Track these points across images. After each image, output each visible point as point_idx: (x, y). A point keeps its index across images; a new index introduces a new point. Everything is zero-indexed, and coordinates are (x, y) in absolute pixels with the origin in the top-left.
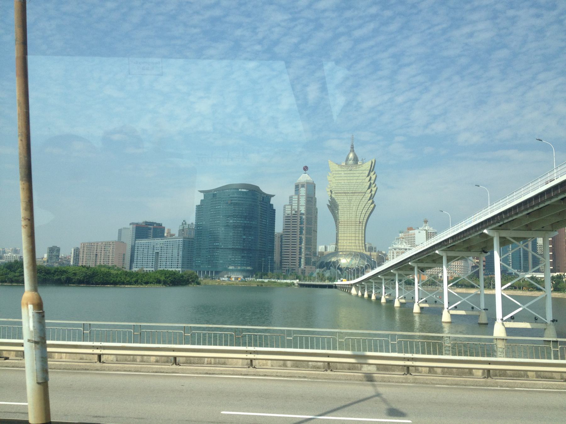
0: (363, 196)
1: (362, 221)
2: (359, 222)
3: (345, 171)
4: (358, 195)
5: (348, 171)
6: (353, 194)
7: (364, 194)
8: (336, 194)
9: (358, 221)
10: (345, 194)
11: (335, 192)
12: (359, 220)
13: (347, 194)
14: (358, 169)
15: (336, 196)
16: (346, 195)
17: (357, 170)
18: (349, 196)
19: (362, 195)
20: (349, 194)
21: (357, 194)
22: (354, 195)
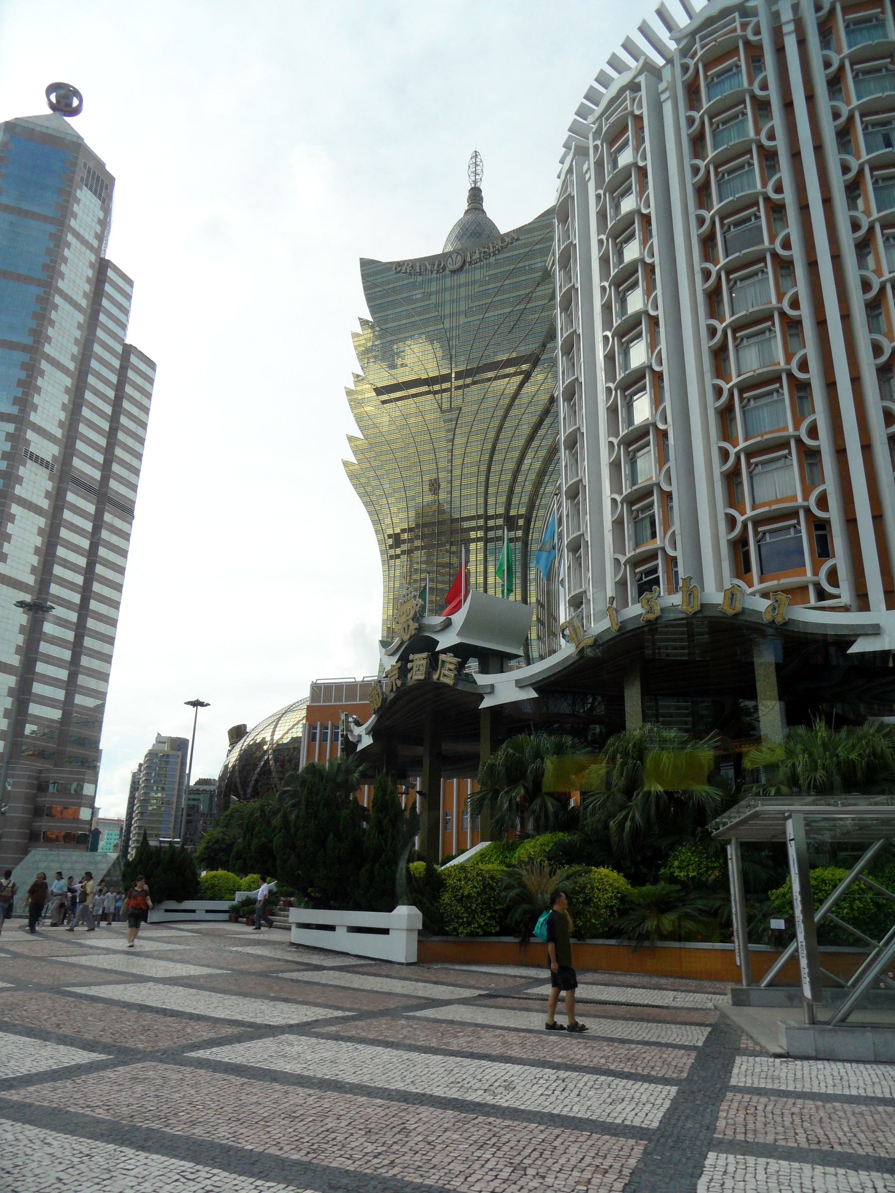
0: (520, 377)
1: (522, 511)
2: (500, 522)
3: (430, 281)
4: (497, 378)
5: (445, 277)
6: (469, 381)
7: (525, 367)
8: (385, 397)
9: (497, 516)
10: (425, 389)
11: (379, 385)
12: (501, 510)
13: (437, 387)
14: (492, 259)
15: (384, 402)
16: (435, 393)
17: (489, 265)
18: (445, 395)
19: (515, 374)
20: (445, 386)
21: (490, 375)
22: (474, 383)
